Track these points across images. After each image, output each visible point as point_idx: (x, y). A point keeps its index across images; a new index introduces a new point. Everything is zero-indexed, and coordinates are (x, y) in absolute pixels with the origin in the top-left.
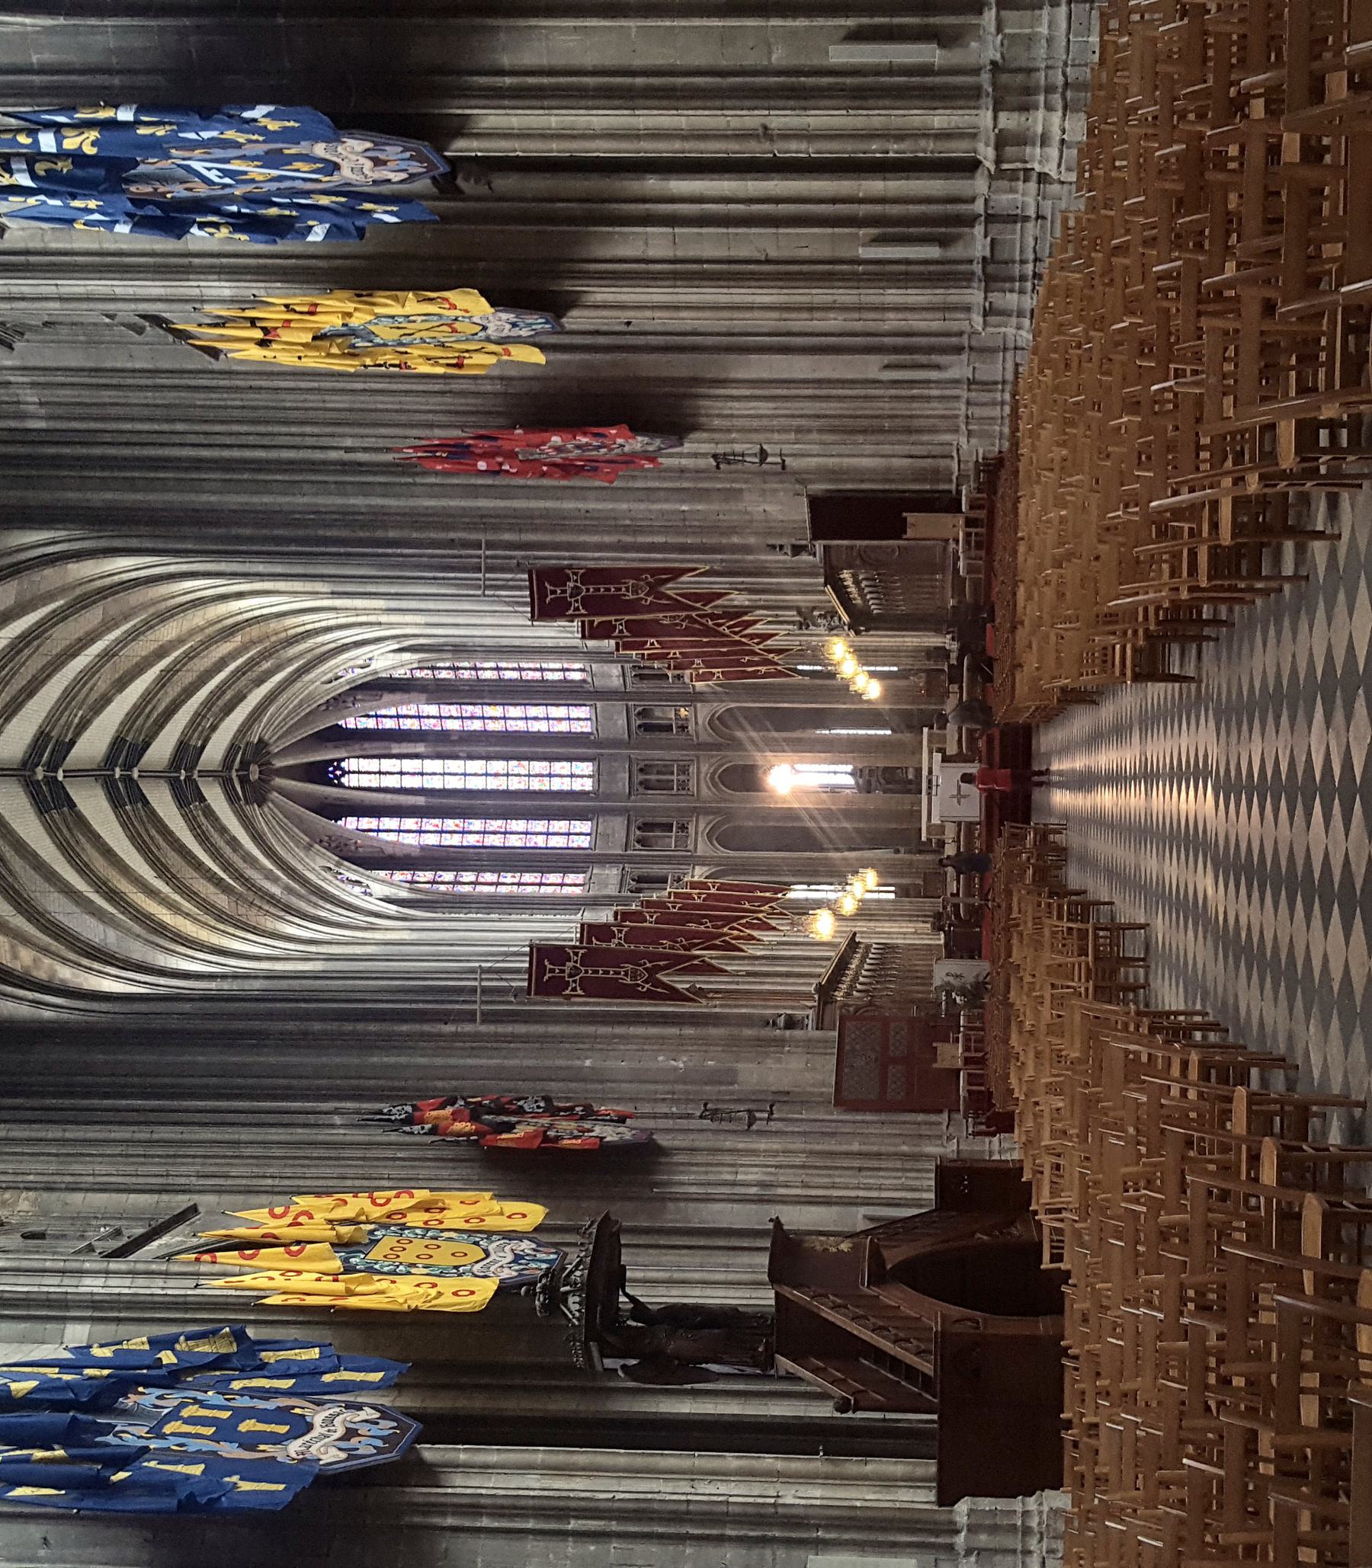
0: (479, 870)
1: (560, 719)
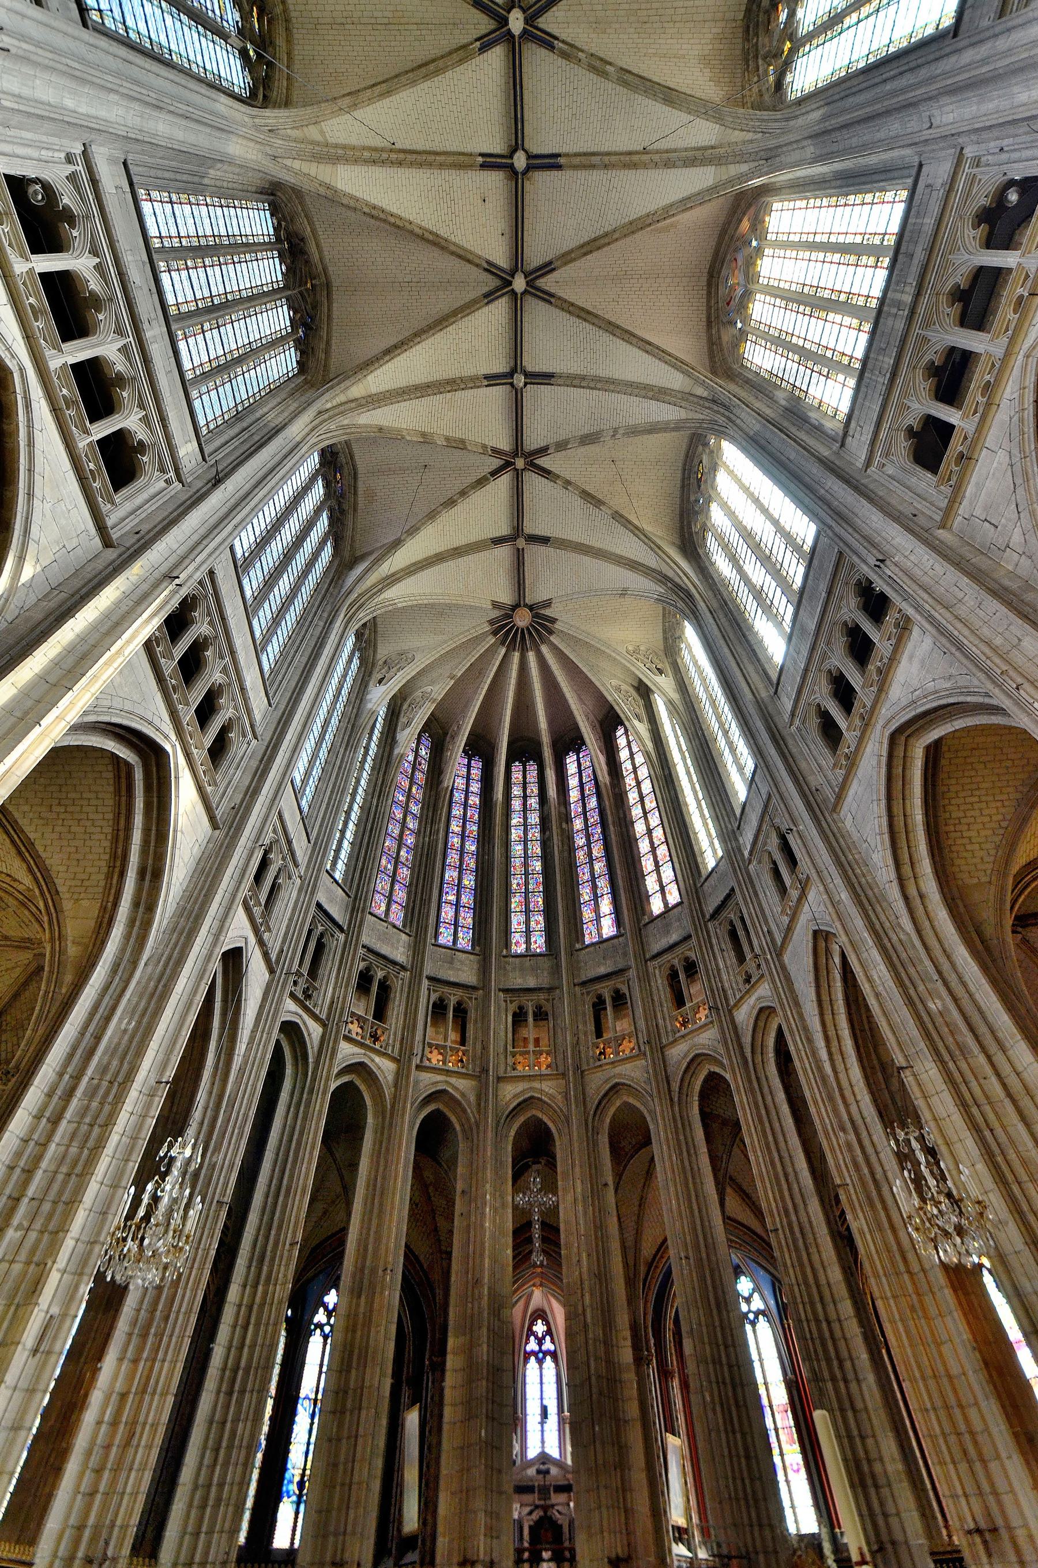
0: (418, 834)
1: (597, 909)
